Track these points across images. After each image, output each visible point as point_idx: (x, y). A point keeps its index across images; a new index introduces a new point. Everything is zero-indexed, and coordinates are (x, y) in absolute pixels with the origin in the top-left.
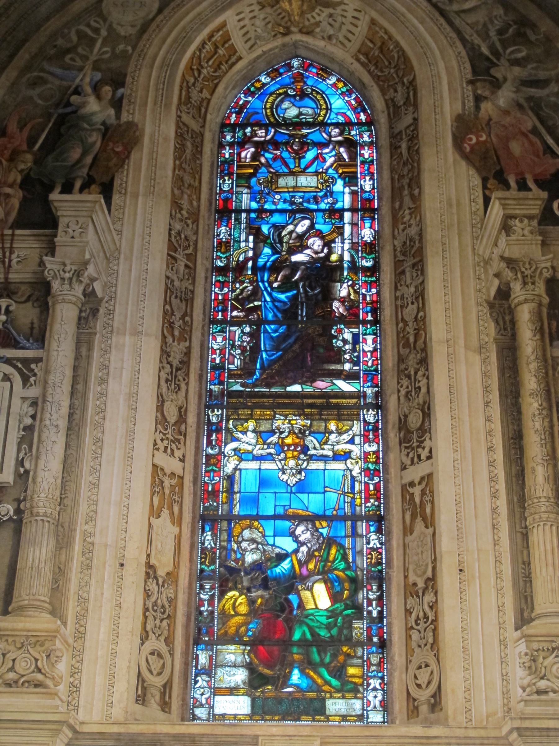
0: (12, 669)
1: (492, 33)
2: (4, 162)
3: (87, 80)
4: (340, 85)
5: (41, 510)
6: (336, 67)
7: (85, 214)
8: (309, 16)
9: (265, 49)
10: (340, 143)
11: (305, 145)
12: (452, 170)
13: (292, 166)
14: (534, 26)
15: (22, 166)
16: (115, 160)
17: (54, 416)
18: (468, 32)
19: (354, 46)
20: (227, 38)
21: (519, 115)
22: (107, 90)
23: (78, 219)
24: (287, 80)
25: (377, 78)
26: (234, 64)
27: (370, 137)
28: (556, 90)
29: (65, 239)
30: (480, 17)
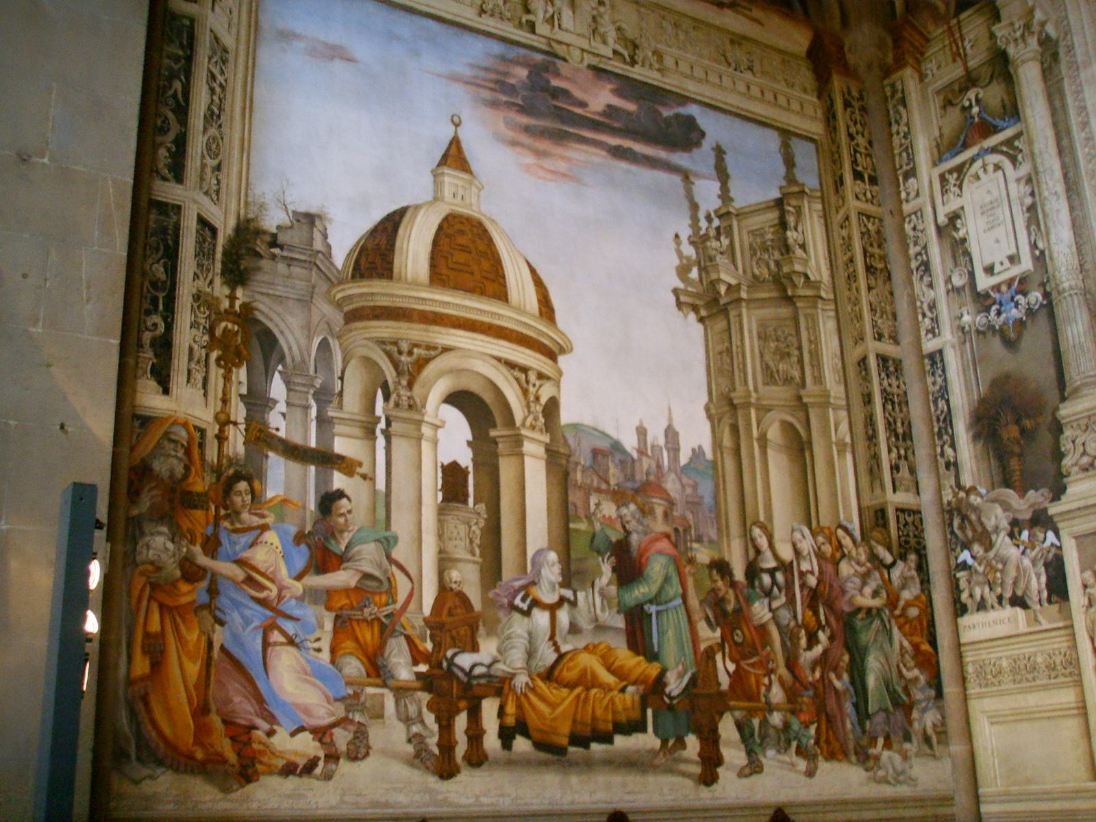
0: (1084, 453)
5: (1066, 285)
17: (1051, 184)
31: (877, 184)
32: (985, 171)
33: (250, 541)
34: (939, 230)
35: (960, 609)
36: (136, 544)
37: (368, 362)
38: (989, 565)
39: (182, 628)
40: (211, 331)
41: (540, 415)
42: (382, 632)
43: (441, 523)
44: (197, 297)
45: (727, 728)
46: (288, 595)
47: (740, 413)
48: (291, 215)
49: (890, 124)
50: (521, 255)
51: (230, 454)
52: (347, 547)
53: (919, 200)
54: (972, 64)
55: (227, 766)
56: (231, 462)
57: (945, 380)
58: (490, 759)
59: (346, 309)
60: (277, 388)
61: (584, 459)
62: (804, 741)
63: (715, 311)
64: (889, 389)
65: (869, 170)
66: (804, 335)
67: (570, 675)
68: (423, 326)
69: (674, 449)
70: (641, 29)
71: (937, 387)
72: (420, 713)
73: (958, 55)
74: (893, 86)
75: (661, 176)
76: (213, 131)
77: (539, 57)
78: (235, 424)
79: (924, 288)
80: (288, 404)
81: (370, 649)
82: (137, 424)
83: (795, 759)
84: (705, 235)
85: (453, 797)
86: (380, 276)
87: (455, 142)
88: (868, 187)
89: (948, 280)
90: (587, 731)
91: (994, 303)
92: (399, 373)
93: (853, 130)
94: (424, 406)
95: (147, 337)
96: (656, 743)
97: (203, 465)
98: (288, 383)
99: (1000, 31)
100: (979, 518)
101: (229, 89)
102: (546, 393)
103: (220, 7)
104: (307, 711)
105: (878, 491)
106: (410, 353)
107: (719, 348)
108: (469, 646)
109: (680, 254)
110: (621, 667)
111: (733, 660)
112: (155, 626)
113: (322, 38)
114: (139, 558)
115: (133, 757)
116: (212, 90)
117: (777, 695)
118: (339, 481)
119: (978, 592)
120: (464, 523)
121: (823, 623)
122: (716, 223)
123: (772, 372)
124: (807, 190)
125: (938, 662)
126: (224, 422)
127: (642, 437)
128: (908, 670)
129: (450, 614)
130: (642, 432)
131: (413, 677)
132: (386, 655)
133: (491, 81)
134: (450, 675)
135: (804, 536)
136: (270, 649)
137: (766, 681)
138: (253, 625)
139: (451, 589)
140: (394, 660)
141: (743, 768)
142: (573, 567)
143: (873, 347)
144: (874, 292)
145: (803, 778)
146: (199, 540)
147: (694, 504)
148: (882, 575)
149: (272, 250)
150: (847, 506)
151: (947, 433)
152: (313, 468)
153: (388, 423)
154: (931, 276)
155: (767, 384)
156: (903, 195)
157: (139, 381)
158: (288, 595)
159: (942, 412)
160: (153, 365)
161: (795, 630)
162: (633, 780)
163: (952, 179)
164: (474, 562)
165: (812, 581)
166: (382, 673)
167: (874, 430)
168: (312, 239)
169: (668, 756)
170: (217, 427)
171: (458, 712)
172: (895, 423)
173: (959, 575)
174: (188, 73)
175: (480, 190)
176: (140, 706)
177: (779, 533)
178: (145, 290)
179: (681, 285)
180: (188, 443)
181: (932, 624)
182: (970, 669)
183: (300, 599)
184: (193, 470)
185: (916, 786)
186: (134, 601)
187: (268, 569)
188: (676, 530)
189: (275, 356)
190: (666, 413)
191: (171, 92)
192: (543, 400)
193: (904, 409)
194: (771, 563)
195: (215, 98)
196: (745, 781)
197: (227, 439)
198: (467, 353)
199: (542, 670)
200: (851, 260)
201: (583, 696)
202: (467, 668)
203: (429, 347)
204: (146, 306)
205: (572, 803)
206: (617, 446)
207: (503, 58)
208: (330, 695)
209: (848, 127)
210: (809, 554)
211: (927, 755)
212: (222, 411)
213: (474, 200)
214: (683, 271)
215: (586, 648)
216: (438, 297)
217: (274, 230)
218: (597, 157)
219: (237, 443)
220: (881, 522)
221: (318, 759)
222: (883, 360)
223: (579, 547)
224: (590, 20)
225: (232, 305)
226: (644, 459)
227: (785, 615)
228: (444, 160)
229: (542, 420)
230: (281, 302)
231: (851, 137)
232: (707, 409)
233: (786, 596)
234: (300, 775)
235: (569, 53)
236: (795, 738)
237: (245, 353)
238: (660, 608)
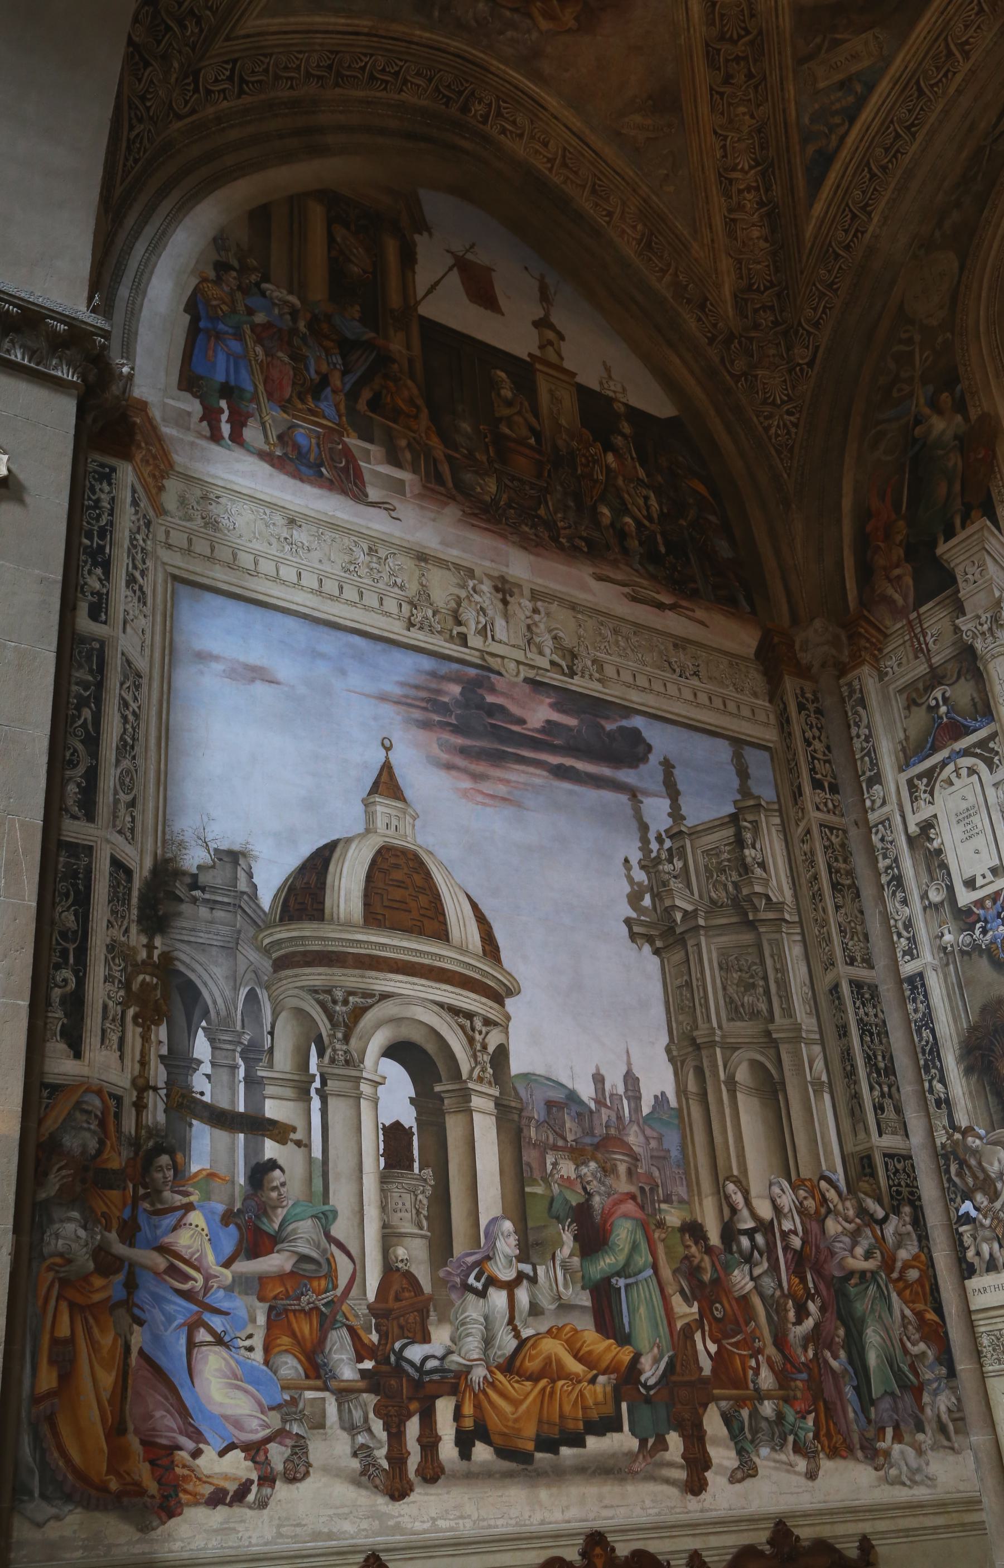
3: (922, 401)
7: (977, 548)
23: (972, 559)
29: (968, 589)
31: (838, 793)
32: (959, 776)
33: (174, 1222)
34: (910, 839)
35: (966, 1270)
36: (43, 1233)
37: (300, 1013)
38: (995, 1217)
39: (96, 1330)
40: (127, 986)
41: (489, 1065)
42: (321, 1325)
43: (384, 1193)
44: (111, 948)
45: (713, 1423)
46: (216, 1285)
47: (704, 1053)
48: (212, 853)
49: (849, 727)
50: (460, 887)
51: (150, 1123)
52: (281, 1225)
53: (886, 809)
54: (936, 660)
55: (146, 1498)
56: (153, 1132)
57: (928, 1006)
58: (446, 1469)
59: (275, 956)
60: (202, 1048)
61: (538, 1113)
62: (801, 1434)
63: (671, 940)
64: (865, 1018)
65: (829, 778)
66: (769, 962)
67: (532, 1365)
68: (357, 972)
69: (636, 1098)
70: (579, 637)
71: (920, 1015)
72: (366, 1419)
73: (921, 651)
74: (850, 685)
75: (608, 796)
76: (126, 763)
77: (472, 672)
78: (155, 1089)
79: (897, 904)
80: (213, 1064)
81: (309, 1345)
82: (45, 1094)
83: (794, 1458)
84: (655, 858)
85: (406, 1522)
86: (312, 918)
87: (387, 768)
88: (828, 796)
89: (924, 896)
90: (555, 1433)
91: (979, 920)
92: (334, 1025)
93: (809, 734)
94: (362, 1062)
95: (57, 993)
96: (634, 1444)
97: (119, 1139)
98: (212, 1041)
99: (965, 624)
100: (980, 1163)
101: (143, 716)
102: (494, 1040)
103: (133, 628)
104: (237, 1423)
105: (862, 1135)
106: (345, 1002)
107: (678, 982)
108: (419, 1336)
109: (630, 880)
110: (590, 1353)
111: (714, 1342)
112: (64, 1330)
113: (242, 658)
114: (46, 1251)
115: (36, 1494)
116: (125, 718)
117: (766, 1379)
118: (271, 1149)
119: (985, 1248)
120: (409, 1191)
121: (813, 1291)
122: (668, 843)
123: (736, 1007)
124: (763, 803)
125: (946, 1333)
126: (143, 1086)
127: (600, 1086)
128: (913, 1345)
129: (397, 1299)
130: (599, 1079)
131: (357, 1377)
132: (327, 1350)
133: (423, 699)
134: (398, 1371)
135: (782, 1190)
136: (196, 1350)
137: (753, 1363)
138: (176, 1323)
139: (398, 1269)
140: (336, 1357)
141: (734, 1471)
142: (531, 1239)
143: (844, 972)
144: (843, 911)
145: (803, 1480)
146: (115, 1225)
147: (660, 1158)
148: (873, 1232)
149: (193, 893)
150: (829, 1154)
151: (935, 1067)
152: (242, 1136)
153: (324, 1082)
154: (904, 892)
155: (733, 1020)
156: (868, 803)
157: (48, 1044)
158: (216, 1285)
159: (927, 1042)
160: (63, 1025)
161: (782, 1301)
162: (609, 1490)
163: (922, 785)
164: (423, 1237)
165: (796, 1242)
166: (322, 1372)
167: (852, 1066)
168: (236, 878)
169: (649, 1460)
170: (135, 1093)
171: (410, 1416)
172: (876, 1058)
173: (961, 1229)
174: (98, 700)
175: (415, 819)
176: (45, 1429)
177: (756, 1186)
178: (54, 942)
179: (634, 915)
180: (102, 1113)
181: (935, 1289)
182: (985, 1341)
183: (229, 1289)
184: (108, 1143)
185: (935, 1486)
186: (40, 1302)
187: (193, 1254)
188: (642, 1189)
189: (197, 1013)
190: (625, 1058)
191: (80, 722)
192: (491, 1049)
193: (884, 1041)
194: (750, 1224)
195: (128, 726)
196: (738, 1486)
197: (146, 1106)
198: (407, 1001)
199: (501, 1360)
200: (815, 877)
201: (548, 1389)
202: (418, 1362)
203: (367, 995)
204: (56, 959)
205: (542, 1523)
206: (572, 1097)
207: (433, 674)
208: (264, 1402)
209: (804, 732)
210: (791, 1210)
211: (945, 1447)
212: (140, 1076)
213: (409, 831)
214: (634, 899)
215: (549, 1332)
216: (373, 939)
217: (194, 871)
218: (538, 778)
219: (157, 1113)
220: (868, 1170)
221: (252, 1482)
222: (857, 985)
223: (537, 1214)
224: (524, 629)
225: (150, 956)
226: (603, 1110)
227: (768, 1284)
228: (375, 788)
229: (490, 1071)
230: (203, 950)
231: (809, 743)
232: (668, 1050)
233: (768, 1260)
234: (230, 1505)
235: (504, 666)
236: (791, 1432)
237: (164, 1008)
238: (630, 1281)
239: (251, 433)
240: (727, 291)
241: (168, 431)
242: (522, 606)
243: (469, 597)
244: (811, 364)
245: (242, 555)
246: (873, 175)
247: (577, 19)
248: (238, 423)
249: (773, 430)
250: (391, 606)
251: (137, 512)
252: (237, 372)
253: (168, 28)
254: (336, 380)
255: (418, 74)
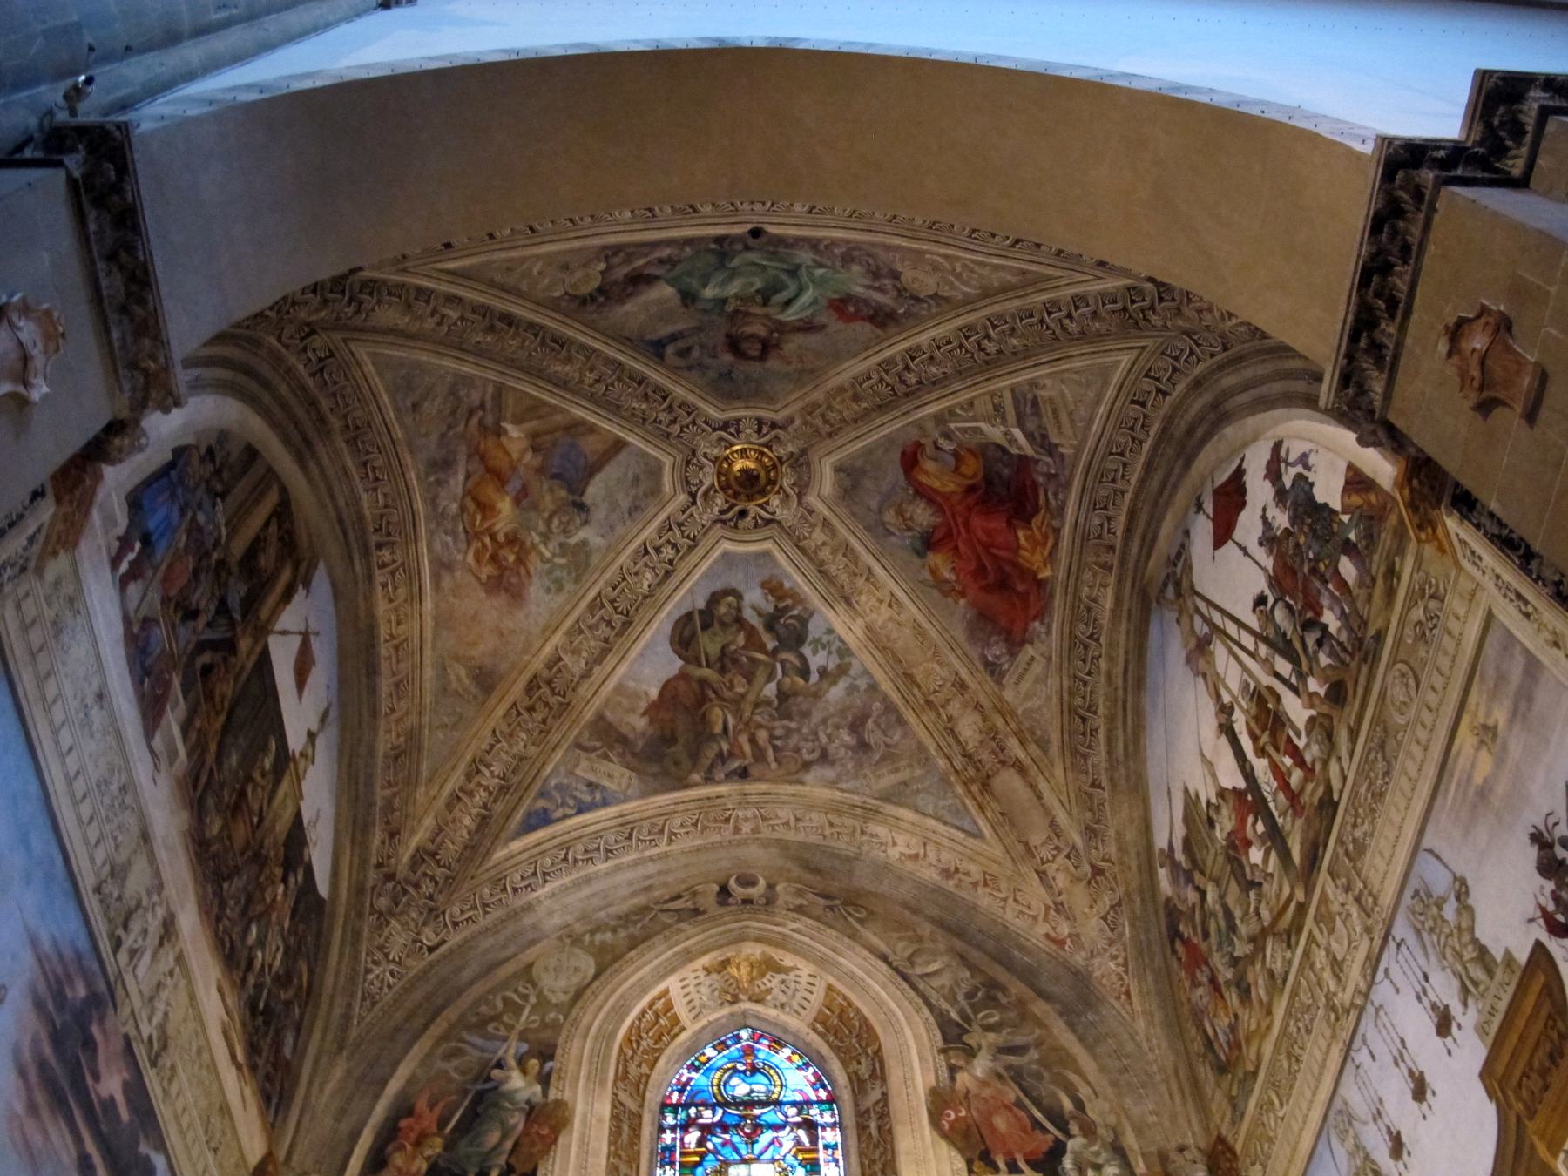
1: (960, 997)
2: (409, 1147)
3: (512, 1051)
4: (796, 1058)
6: (789, 1038)
8: (759, 982)
9: (711, 1018)
10: (799, 1125)
11: (758, 1128)
12: (931, 1152)
13: (744, 1152)
14: (1004, 989)
15: (428, 1152)
16: (538, 1147)
18: (934, 997)
19: (810, 1014)
20: (669, 1006)
21: (999, 1085)
22: (534, 1063)
24: (736, 1054)
25: (836, 1050)
26: (676, 1035)
27: (833, 1115)
28: (1037, 1056)
30: (945, 980)
207: (79, 957)
239: (134, 589)
240: (414, 843)
241: (96, 516)
242: (168, 960)
243: (146, 909)
244: (431, 950)
245: (52, 681)
246: (566, 859)
247: (489, 577)
248: (134, 574)
249: (370, 976)
250: (100, 855)
251: (25, 549)
252: (162, 535)
253: (343, 292)
254: (202, 620)
255: (385, 495)
